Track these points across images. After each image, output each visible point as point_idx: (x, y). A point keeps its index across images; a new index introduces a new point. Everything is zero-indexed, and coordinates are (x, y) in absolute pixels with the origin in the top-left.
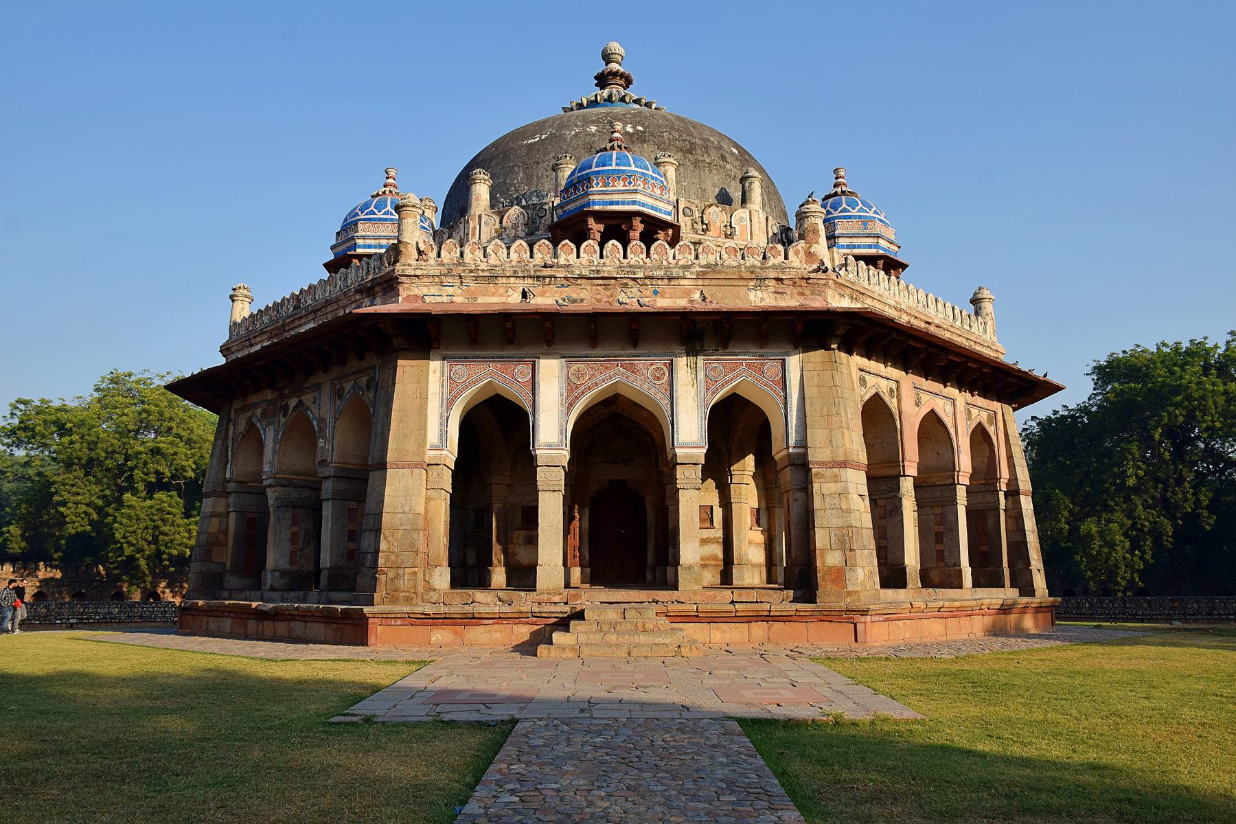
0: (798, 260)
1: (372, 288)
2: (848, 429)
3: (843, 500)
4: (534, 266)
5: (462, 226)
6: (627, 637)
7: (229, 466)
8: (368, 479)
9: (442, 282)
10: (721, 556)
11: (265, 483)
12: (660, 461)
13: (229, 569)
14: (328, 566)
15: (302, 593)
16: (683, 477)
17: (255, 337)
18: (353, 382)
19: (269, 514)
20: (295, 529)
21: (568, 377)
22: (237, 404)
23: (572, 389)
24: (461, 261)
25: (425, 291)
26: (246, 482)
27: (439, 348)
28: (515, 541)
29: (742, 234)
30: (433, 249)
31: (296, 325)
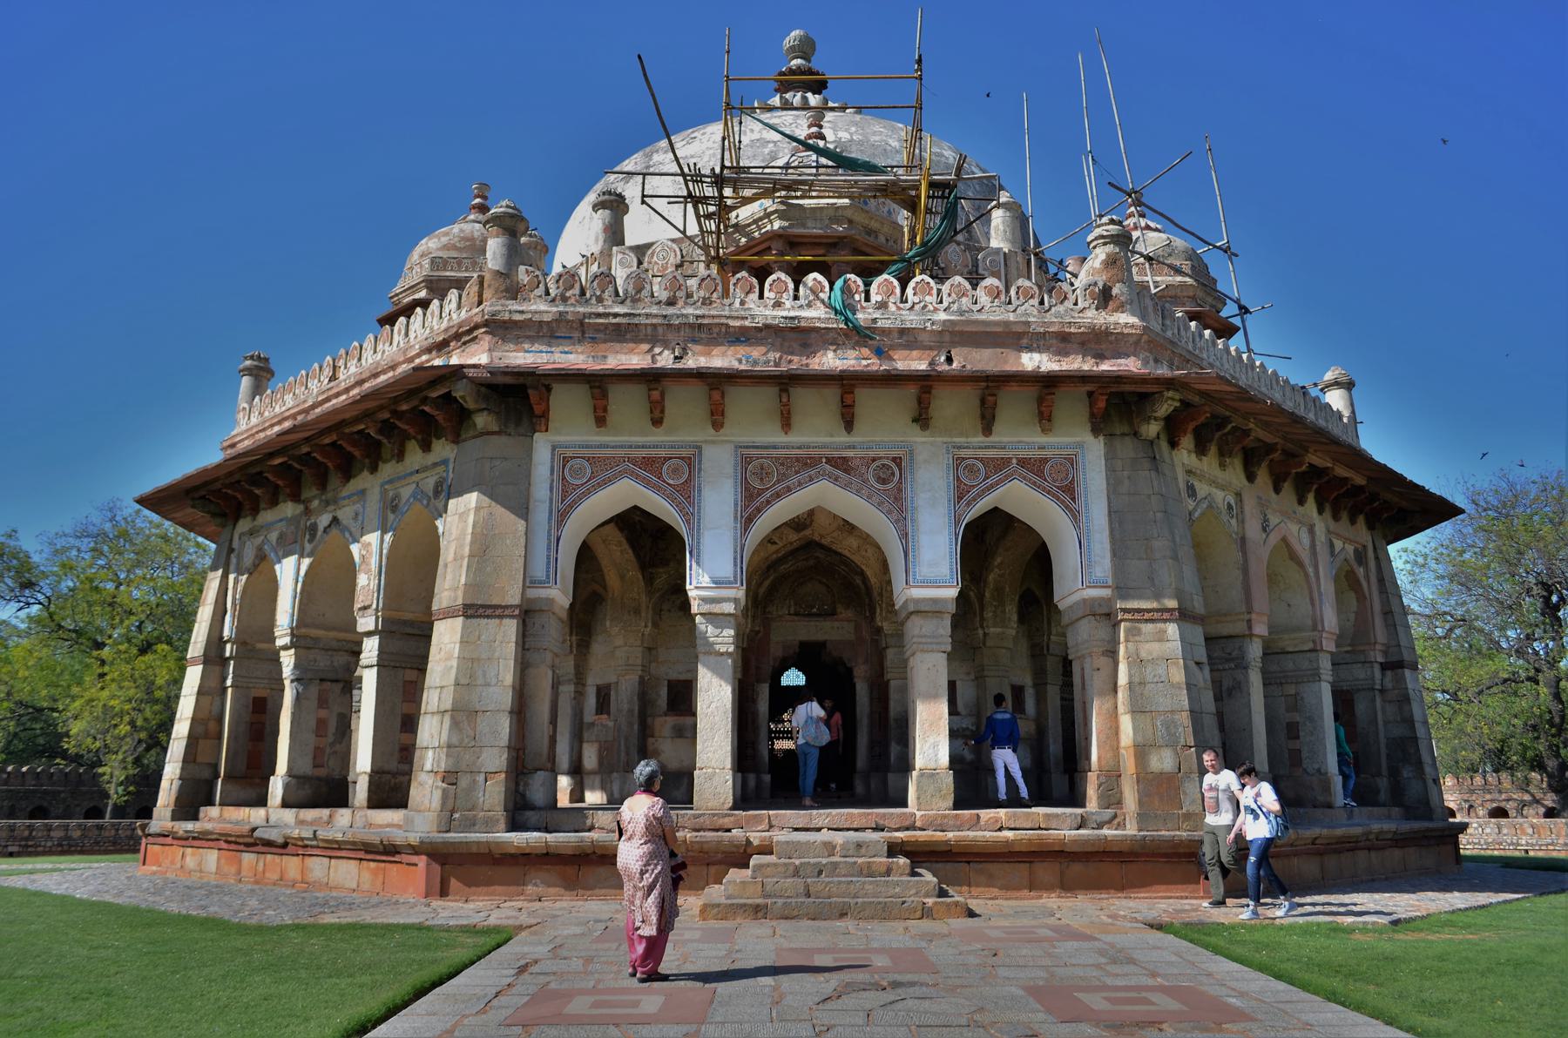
2: (1175, 558)
6: (843, 886)
7: (228, 618)
12: (878, 610)
14: (368, 769)
15: (325, 812)
18: (414, 485)
19: (283, 690)
22: (244, 525)
23: (751, 496)
27: (547, 431)
28: (657, 734)
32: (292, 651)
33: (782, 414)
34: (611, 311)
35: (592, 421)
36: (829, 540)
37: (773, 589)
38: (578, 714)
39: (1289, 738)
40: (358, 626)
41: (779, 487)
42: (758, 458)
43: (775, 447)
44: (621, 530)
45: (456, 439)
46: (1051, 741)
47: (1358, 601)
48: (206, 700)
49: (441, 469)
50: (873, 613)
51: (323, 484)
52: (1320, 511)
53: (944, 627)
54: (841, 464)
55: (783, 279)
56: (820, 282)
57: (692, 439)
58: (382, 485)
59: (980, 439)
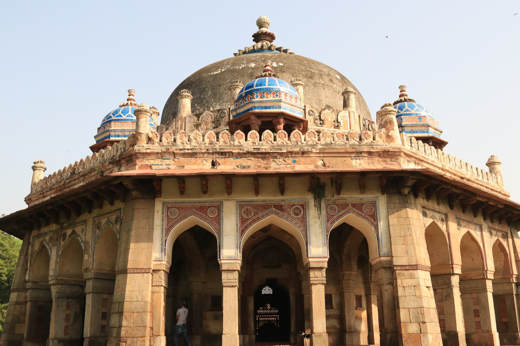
0: (382, 140)
1: (119, 161)
3: (417, 290)
4: (219, 146)
5: (174, 123)
7: (28, 272)
8: (115, 280)
9: (163, 157)
10: (338, 326)
11: (50, 283)
13: (25, 338)
14: (89, 336)
16: (314, 276)
17: (47, 192)
19: (52, 302)
20: (68, 312)
21: (241, 214)
22: (34, 233)
24: (174, 144)
25: (152, 162)
26: (38, 282)
27: (160, 197)
29: (344, 126)
30: (157, 136)
31: (72, 184)
32: (56, 286)
33: (255, 188)
34: (186, 148)
35: (178, 192)
39: (475, 317)
40: (84, 276)
41: (254, 218)
42: (246, 206)
43: (252, 201)
45: (124, 200)
47: (504, 256)
48: (18, 307)
49: (118, 212)
51: (68, 217)
52: (485, 220)
54: (279, 207)
55: (255, 133)
56: (269, 134)
57: (219, 199)
58: (94, 218)
59: (336, 197)
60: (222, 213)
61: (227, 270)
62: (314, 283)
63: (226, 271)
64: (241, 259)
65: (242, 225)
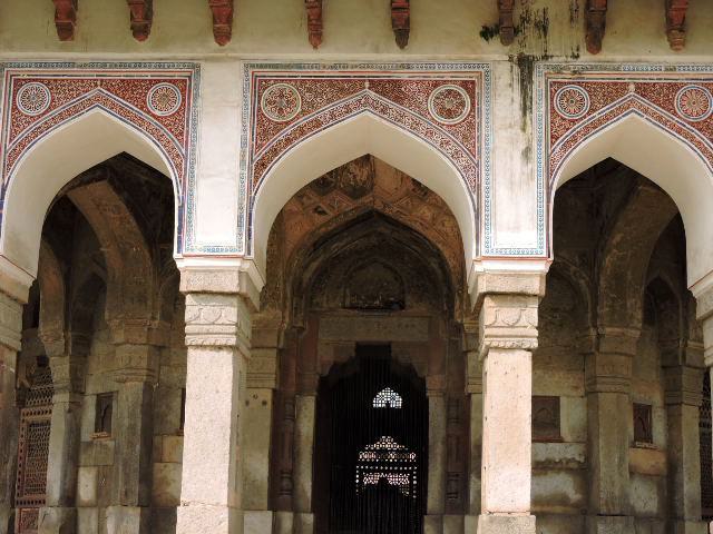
10: (574, 496)
12: (457, 303)
33: (309, 20)
35: (53, 31)
36: (396, 209)
37: (322, 273)
38: (74, 431)
41: (302, 121)
43: (299, 66)
44: (118, 190)
46: (686, 479)
50: (451, 307)
53: (531, 315)
54: (391, 89)
59: (586, 58)
60: (195, 101)
61: (204, 292)
62: (494, 344)
63: (201, 296)
64: (252, 256)
65: (262, 146)
